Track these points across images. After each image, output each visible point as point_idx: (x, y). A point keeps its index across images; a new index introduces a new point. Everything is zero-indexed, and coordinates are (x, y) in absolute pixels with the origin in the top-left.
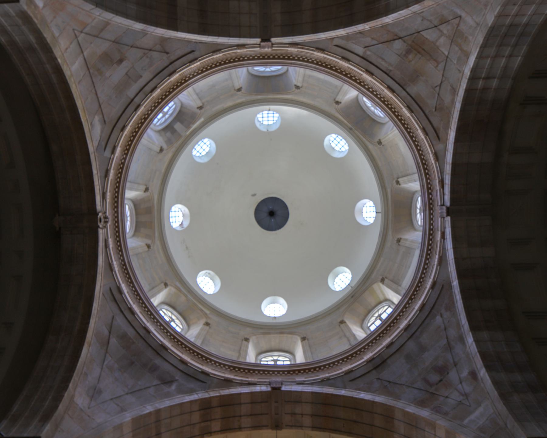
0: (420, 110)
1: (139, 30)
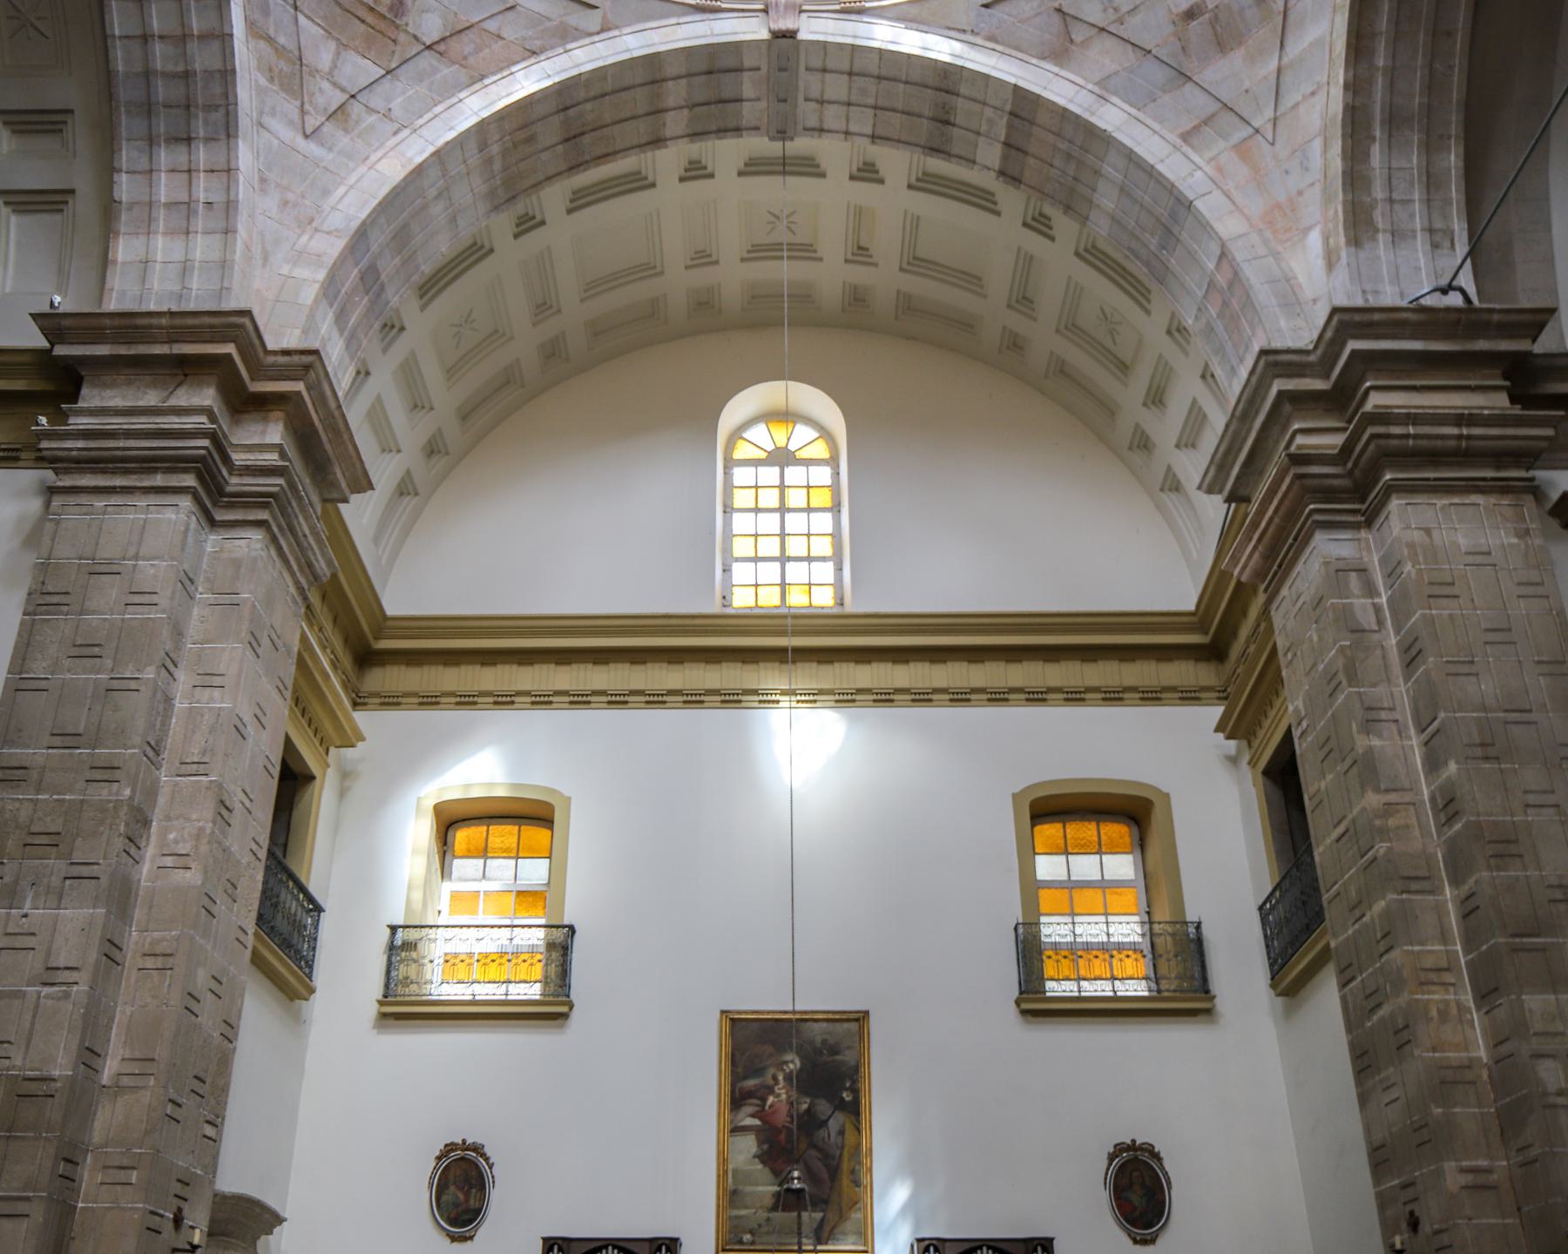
1: (1114, 99)
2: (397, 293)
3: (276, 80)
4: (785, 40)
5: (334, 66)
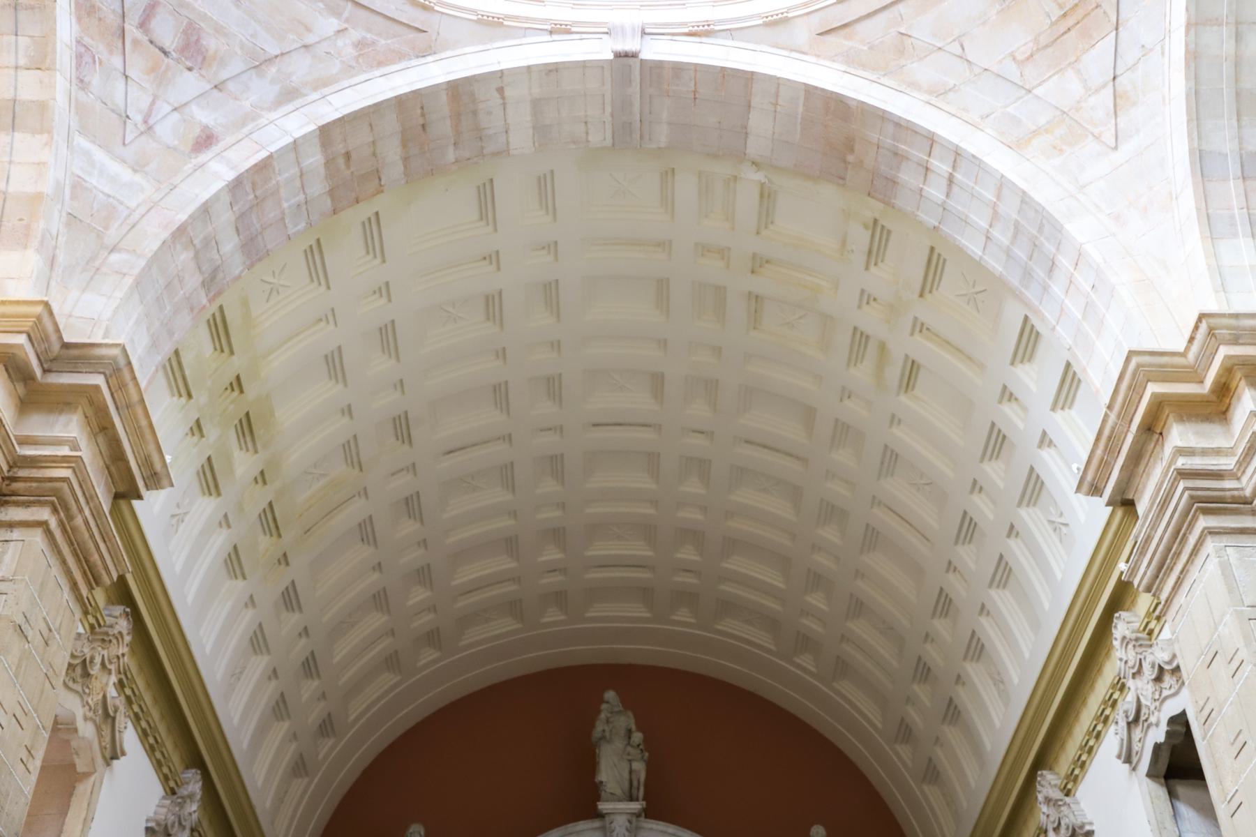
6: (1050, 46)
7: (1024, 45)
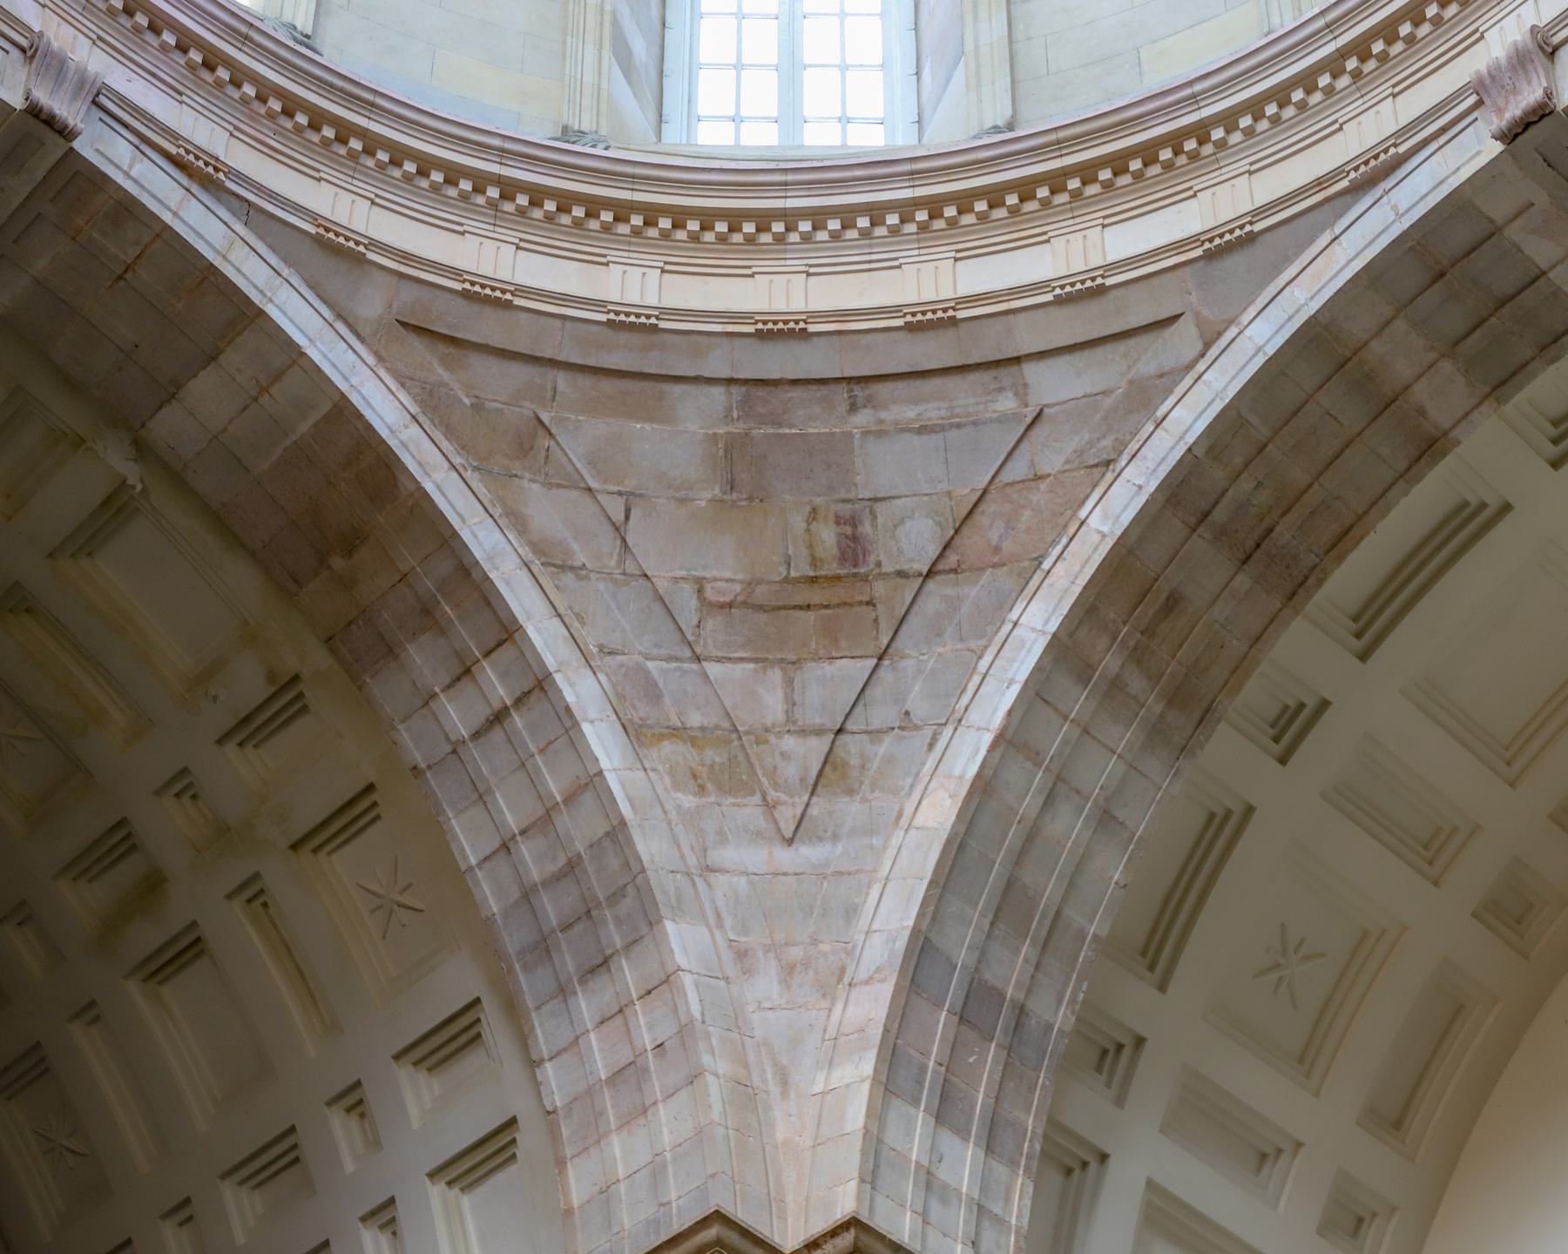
0: (591, 362)
2: (1059, 1003)
3: (709, 785)
4: (1533, 130)
5: (791, 704)
6: (765, 611)
7: (727, 581)
